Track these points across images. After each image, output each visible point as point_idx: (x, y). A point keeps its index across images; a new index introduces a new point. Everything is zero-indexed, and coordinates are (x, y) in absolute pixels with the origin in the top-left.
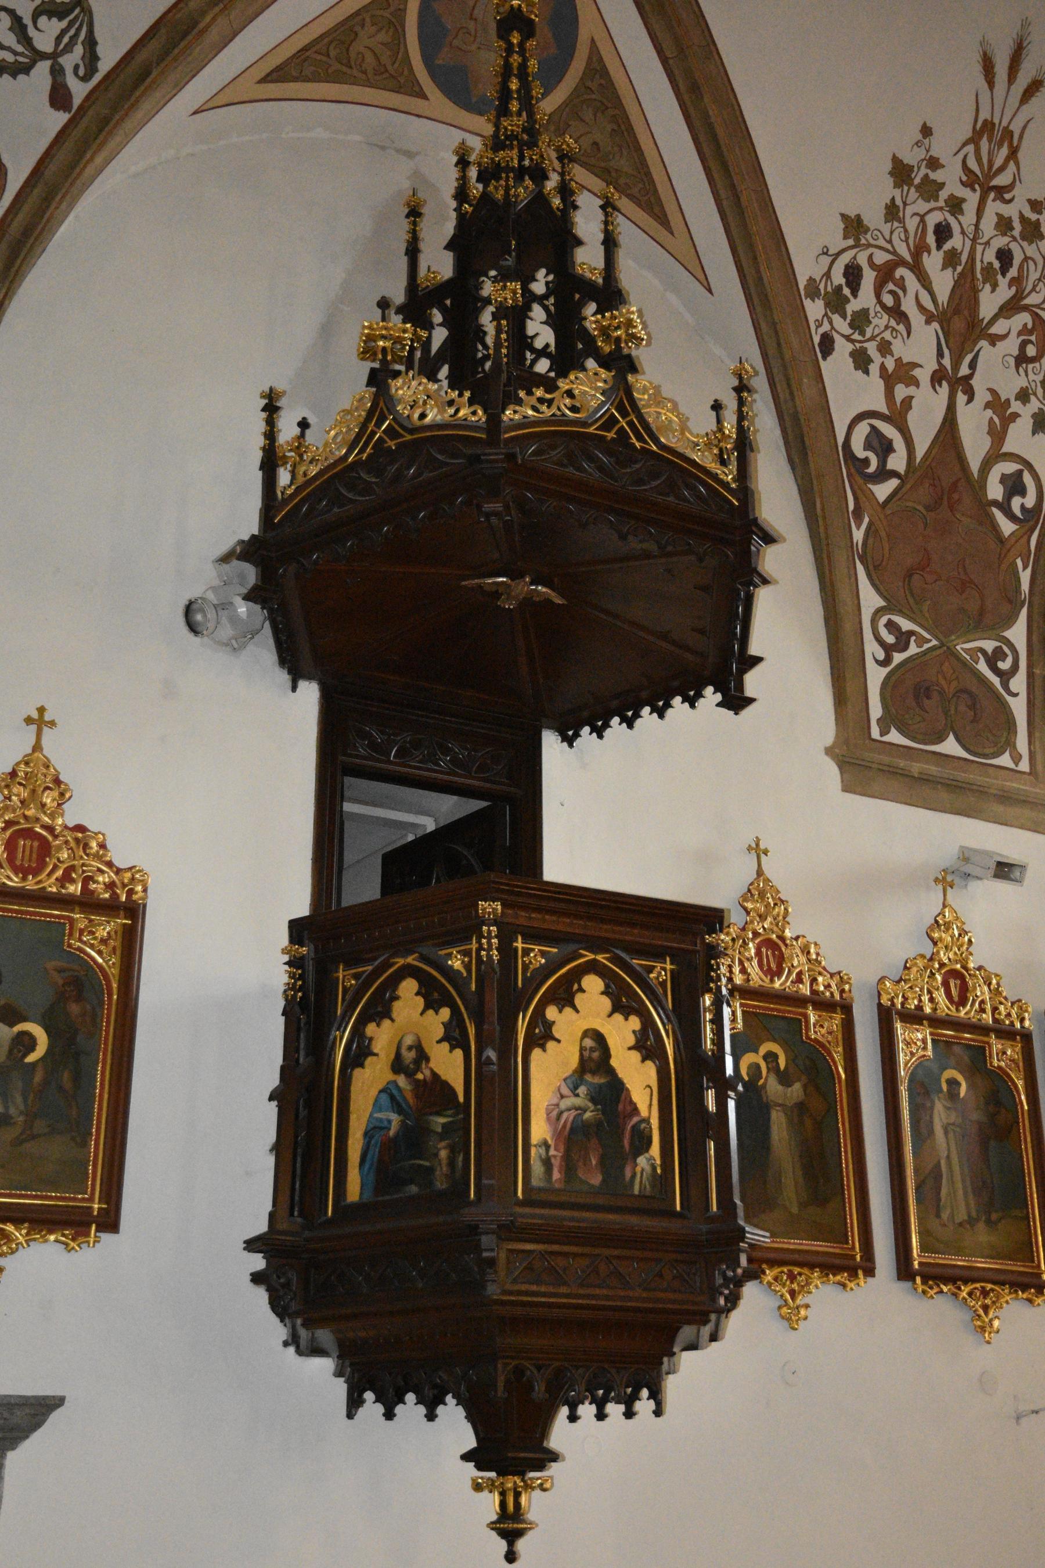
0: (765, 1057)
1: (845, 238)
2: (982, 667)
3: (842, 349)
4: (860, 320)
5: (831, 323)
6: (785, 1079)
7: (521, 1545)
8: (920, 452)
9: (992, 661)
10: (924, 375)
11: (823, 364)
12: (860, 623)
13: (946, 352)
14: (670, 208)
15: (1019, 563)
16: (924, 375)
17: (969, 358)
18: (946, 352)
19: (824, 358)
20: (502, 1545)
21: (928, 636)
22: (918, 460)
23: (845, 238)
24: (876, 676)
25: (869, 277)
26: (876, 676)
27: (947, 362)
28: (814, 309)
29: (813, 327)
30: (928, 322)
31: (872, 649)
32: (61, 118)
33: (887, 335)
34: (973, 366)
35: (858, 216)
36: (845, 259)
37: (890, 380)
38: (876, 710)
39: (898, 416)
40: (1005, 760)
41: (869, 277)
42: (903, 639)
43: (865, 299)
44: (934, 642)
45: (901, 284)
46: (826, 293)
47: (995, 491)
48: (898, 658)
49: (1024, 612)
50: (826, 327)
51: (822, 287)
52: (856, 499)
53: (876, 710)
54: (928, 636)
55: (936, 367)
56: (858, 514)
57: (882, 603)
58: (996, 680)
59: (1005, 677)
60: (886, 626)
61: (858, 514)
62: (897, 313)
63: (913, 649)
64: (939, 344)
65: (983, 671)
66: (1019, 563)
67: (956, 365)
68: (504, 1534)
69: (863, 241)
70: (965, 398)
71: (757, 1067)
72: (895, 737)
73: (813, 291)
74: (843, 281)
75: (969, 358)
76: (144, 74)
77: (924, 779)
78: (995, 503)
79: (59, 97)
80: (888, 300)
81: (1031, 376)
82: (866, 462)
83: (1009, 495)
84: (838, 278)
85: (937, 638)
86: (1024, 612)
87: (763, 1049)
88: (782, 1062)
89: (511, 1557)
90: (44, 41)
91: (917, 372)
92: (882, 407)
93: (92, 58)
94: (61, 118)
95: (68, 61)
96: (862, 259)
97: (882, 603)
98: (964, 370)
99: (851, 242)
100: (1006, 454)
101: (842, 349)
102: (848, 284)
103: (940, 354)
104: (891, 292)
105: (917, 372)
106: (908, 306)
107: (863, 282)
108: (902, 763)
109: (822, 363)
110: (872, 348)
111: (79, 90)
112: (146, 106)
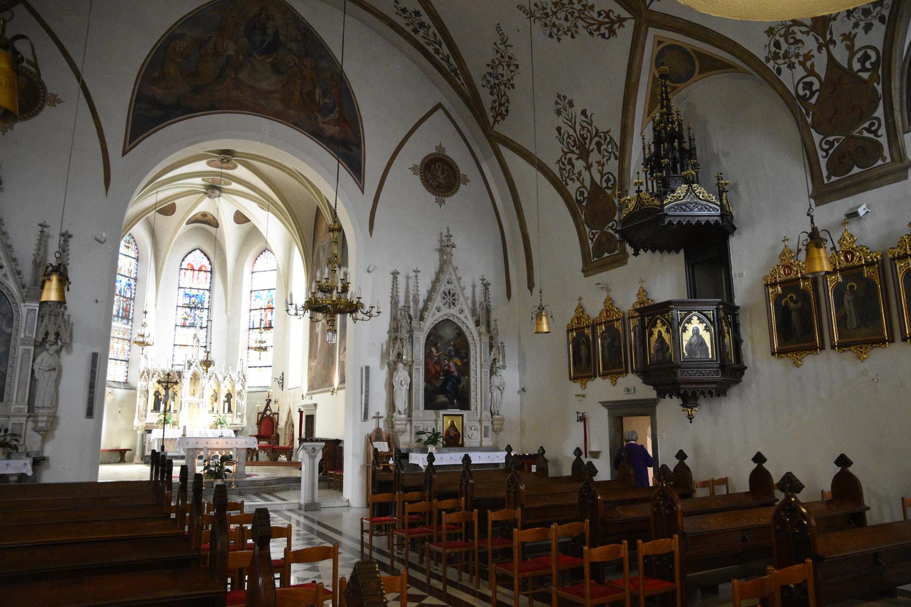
0: (789, 298)
1: (769, 37)
2: (865, 134)
3: (784, 68)
4: (786, 55)
5: (777, 64)
6: (795, 302)
7: (692, 420)
8: (823, 76)
9: (869, 130)
10: (814, 52)
11: (780, 78)
12: (815, 148)
13: (819, 38)
14: (735, 65)
15: (875, 84)
16: (814, 52)
17: (828, 32)
18: (819, 38)
19: (780, 75)
20: (689, 420)
21: (841, 137)
22: (823, 79)
23: (769, 37)
24: (823, 163)
25: (782, 40)
26: (823, 163)
27: (821, 41)
28: (771, 65)
29: (772, 69)
30: (808, 35)
31: (821, 154)
32: (618, 160)
33: (797, 51)
34: (831, 33)
35: (770, 28)
36: (772, 42)
37: (802, 64)
38: (825, 173)
39: (811, 72)
40: (880, 162)
41: (782, 40)
42: (831, 144)
43: (784, 46)
44: (844, 137)
45: (794, 33)
46: (772, 57)
47: (856, 66)
48: (831, 152)
49: (881, 102)
50: (776, 66)
51: (770, 57)
52: (806, 109)
53: (825, 173)
54: (841, 137)
55: (818, 45)
56: (808, 114)
57: (822, 137)
58: (872, 136)
59: (875, 133)
60: (825, 144)
61: (808, 114)
62: (797, 41)
63: (836, 145)
64: (815, 37)
65: (866, 136)
66: (875, 84)
67: (824, 38)
68: (689, 418)
69: (775, 32)
70: (833, 46)
71: (787, 301)
72: (833, 179)
73: (768, 59)
74: (775, 49)
75: (828, 32)
76: (624, 142)
77: (846, 187)
78: (859, 71)
79: (616, 158)
80: (792, 41)
81: (856, 16)
82: (806, 94)
83: (863, 65)
84: (773, 49)
85: (844, 136)
86: (881, 102)
87: (788, 296)
88: (795, 298)
89: (691, 422)
90: (610, 150)
91: (811, 53)
92: (805, 74)
93: (617, 146)
94: (618, 160)
95: (614, 150)
96: (777, 37)
97: (822, 137)
98: (828, 37)
99: (771, 36)
100: (857, 51)
101: (784, 68)
102: (777, 49)
103: (817, 40)
104: (791, 38)
105: (811, 53)
106: (799, 36)
107: (781, 44)
108: (837, 187)
109: (780, 77)
110: (793, 60)
111: (617, 153)
112: (628, 147)
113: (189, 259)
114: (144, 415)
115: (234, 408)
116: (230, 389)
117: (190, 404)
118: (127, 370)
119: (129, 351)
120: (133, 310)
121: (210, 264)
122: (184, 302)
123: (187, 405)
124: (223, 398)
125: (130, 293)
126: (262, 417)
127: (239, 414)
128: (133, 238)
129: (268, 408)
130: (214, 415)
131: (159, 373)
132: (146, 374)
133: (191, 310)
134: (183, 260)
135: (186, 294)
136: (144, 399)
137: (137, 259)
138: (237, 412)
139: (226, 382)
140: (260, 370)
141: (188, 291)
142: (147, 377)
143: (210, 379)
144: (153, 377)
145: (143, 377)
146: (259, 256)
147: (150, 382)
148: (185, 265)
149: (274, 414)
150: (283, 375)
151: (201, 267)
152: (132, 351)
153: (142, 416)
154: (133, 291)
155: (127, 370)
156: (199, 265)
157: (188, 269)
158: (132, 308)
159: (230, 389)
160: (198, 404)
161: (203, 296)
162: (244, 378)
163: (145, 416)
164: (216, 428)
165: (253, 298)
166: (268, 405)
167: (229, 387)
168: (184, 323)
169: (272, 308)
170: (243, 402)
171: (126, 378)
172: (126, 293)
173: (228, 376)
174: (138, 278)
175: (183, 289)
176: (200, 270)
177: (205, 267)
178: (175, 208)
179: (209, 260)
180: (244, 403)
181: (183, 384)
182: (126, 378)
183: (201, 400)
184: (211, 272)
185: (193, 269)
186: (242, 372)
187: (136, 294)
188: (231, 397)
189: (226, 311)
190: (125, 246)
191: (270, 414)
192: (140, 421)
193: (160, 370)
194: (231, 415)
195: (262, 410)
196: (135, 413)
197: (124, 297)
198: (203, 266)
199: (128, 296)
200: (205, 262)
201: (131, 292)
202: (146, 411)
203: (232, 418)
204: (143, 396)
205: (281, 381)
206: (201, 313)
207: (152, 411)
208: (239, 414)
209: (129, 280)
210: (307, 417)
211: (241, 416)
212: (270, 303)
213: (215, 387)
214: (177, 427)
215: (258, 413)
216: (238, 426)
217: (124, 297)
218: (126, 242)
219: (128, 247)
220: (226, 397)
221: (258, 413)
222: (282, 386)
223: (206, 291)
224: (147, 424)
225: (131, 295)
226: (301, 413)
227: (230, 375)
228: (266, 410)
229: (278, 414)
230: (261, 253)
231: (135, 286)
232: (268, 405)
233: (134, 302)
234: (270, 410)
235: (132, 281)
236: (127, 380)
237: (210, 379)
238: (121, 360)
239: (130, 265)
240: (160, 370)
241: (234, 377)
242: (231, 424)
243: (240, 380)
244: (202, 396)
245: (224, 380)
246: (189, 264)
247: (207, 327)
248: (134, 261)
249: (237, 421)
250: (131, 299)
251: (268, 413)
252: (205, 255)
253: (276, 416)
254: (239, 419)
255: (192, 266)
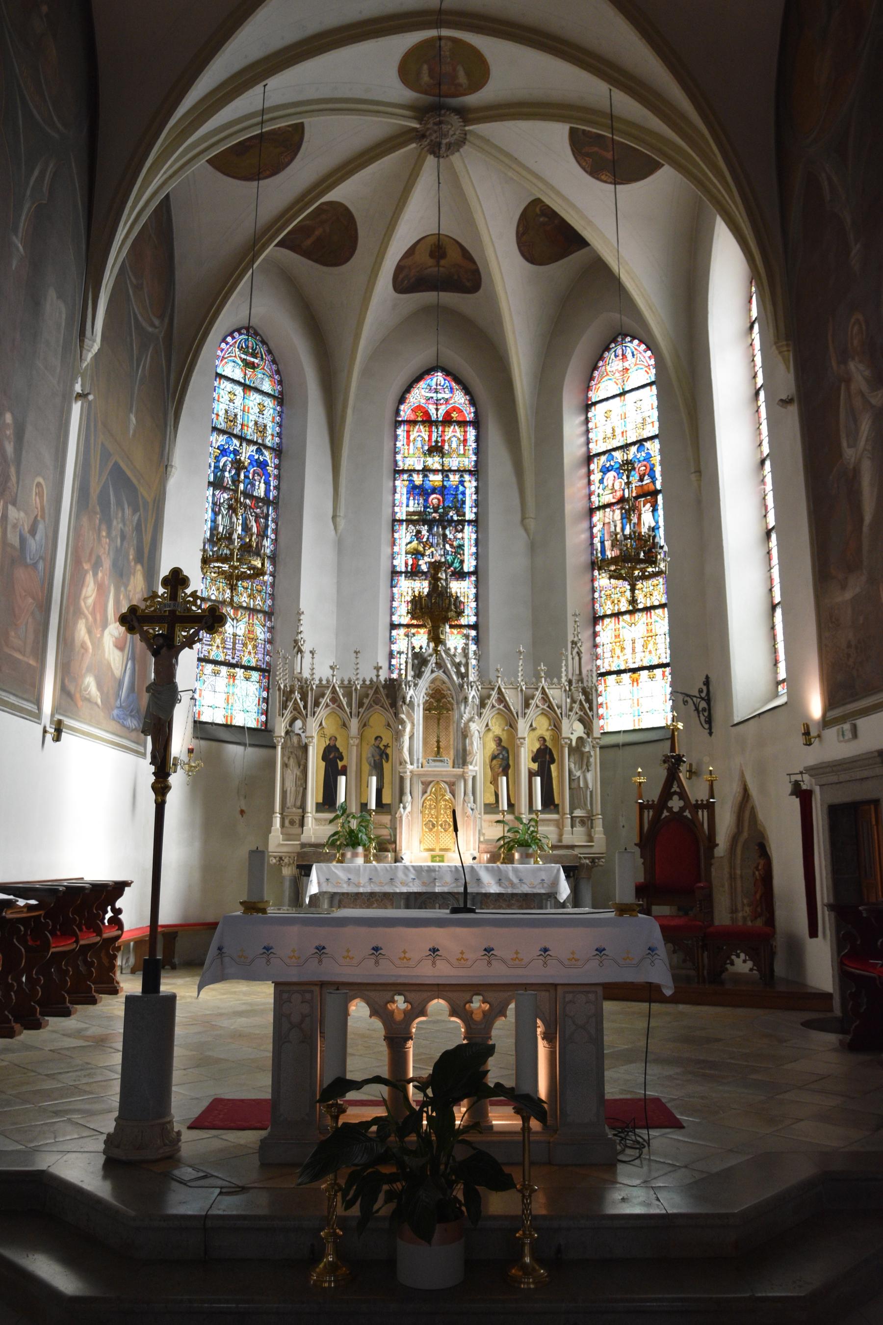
113: (419, 395)
114: (297, 819)
115: (562, 795)
116: (547, 736)
117: (426, 784)
118: (265, 694)
119: (270, 642)
120: (276, 531)
121: (473, 402)
122: (411, 509)
123: (418, 788)
124: (525, 762)
125: (263, 486)
126: (656, 821)
127: (578, 813)
128: (263, 342)
129: (675, 788)
130: (500, 817)
131: (334, 691)
132: (297, 696)
133: (430, 531)
134: (402, 400)
135: (415, 487)
136: (293, 773)
137: (280, 400)
138: (572, 809)
139: (531, 711)
140: (635, 681)
141: (418, 479)
142: (301, 705)
143: (483, 705)
144: (317, 704)
145: (290, 704)
146: (601, 358)
147: (310, 720)
148: (406, 412)
149: (698, 806)
150: (707, 682)
151: (448, 414)
152: (278, 639)
153: (292, 823)
154: (273, 483)
155: (265, 694)
156: (443, 410)
157: (414, 423)
158: (272, 525)
159: (547, 736)
160: (452, 785)
161: (461, 488)
162: (589, 701)
163: (302, 824)
164: (509, 860)
165: (596, 477)
166: (672, 776)
167: (543, 727)
168: (416, 566)
169: (655, 493)
170: (589, 776)
171: (263, 718)
172: (253, 485)
173: (538, 694)
174: (284, 449)
175: (405, 476)
176: (447, 421)
177: (460, 411)
178: (356, 230)
179: (467, 391)
180: (592, 779)
181: (402, 722)
182: (263, 718)
183: (459, 771)
184: (476, 423)
185: (428, 421)
186: (581, 680)
187: (283, 486)
188: (553, 761)
189: (523, 519)
190: (243, 360)
191: (682, 809)
192: (288, 836)
193: (336, 682)
194: (555, 816)
195: (653, 794)
196: (274, 812)
197: (246, 495)
198: (454, 409)
199: (260, 491)
200: (460, 399)
201: (267, 483)
202: (303, 807)
203: (559, 825)
204: (292, 762)
205: (703, 705)
206: (459, 535)
207: (319, 808)
208: (578, 813)
209: (259, 451)
210: (834, 811)
211: (587, 822)
212: (647, 480)
213: (497, 729)
214: (390, 855)
215: (642, 807)
216: (576, 852)
217: (246, 495)
218: (246, 353)
219: (253, 366)
220: (534, 760)
221: (642, 807)
222: (709, 721)
223: (467, 477)
224: (303, 845)
225: (267, 491)
226: (804, 797)
227: (544, 692)
228: (666, 794)
229: (710, 807)
230: (607, 349)
231: (277, 467)
232: (672, 776)
233: (276, 509)
234: (683, 795)
235: (268, 456)
236: (266, 723)
237: (483, 705)
238: (247, 668)
239: (261, 412)
240: (336, 682)
241: (556, 695)
242: (554, 847)
243: (576, 706)
244: (463, 758)
245: (527, 705)
246: (419, 408)
247: (475, 573)
248: (269, 403)
249: (575, 836)
250: (266, 501)
251: (675, 804)
252: (458, 381)
253: (703, 815)
254: (579, 829)
255: (426, 413)
